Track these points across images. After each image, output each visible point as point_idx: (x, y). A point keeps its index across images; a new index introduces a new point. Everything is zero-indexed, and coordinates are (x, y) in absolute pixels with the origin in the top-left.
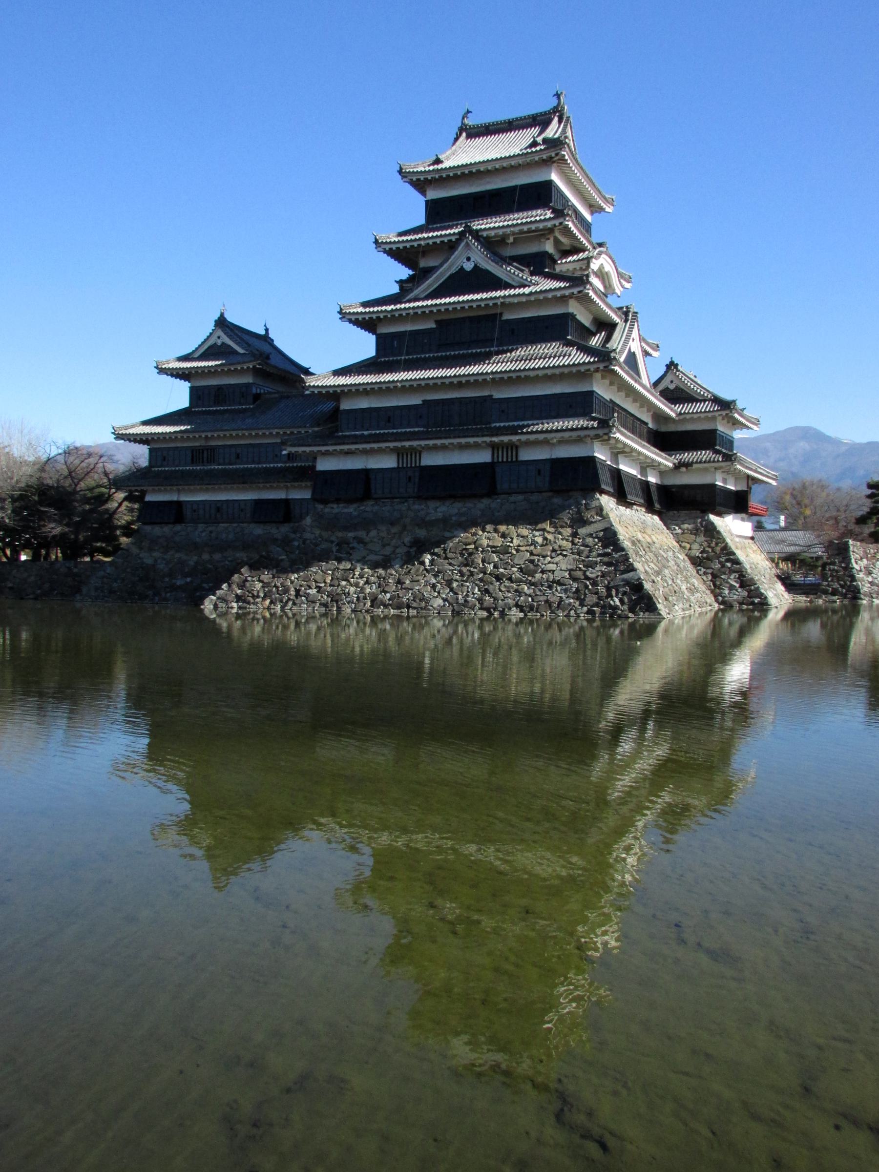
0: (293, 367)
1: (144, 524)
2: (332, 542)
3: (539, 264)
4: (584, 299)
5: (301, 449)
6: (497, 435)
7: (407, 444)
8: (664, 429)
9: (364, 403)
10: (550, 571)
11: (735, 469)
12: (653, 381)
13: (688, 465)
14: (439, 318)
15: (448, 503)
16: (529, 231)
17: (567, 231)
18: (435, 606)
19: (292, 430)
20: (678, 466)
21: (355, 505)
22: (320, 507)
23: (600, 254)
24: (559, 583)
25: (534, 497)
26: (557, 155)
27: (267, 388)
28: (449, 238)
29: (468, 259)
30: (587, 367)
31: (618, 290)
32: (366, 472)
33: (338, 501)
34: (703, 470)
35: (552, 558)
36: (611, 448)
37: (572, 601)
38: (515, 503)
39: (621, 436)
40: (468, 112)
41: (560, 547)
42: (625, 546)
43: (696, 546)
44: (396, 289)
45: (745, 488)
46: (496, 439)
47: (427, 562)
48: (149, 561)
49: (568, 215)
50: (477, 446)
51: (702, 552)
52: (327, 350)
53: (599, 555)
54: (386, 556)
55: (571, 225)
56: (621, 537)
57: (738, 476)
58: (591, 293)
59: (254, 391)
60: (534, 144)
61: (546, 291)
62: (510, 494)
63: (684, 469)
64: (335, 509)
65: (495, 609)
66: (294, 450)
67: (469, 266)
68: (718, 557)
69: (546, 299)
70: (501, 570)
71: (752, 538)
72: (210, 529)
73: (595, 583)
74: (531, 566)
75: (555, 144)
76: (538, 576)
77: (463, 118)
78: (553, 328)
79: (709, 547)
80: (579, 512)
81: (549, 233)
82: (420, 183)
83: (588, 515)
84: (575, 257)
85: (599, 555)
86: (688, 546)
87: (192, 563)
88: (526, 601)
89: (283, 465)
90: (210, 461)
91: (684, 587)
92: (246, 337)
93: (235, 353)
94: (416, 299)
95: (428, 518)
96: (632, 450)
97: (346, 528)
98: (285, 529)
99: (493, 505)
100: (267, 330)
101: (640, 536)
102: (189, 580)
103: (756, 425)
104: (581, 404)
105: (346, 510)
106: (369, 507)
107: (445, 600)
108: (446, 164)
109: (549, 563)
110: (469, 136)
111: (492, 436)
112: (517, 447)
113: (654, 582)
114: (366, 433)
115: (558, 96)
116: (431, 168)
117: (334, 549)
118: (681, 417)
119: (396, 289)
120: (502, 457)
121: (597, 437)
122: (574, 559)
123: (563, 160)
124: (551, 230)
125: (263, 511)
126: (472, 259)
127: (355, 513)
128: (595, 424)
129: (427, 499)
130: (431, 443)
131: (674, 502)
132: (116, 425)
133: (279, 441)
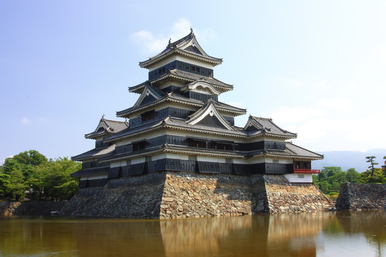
14: (142, 113)
21: (117, 180)
24: (144, 206)
25: (155, 174)
26: (174, 52)
32: (121, 168)
38: (150, 176)
40: (171, 39)
45: (292, 163)
48: (77, 200)
50: (140, 157)
66: (102, 161)
67: (148, 94)
82: (147, 67)
86: (254, 188)
105: (115, 181)
106: (121, 180)
111: (139, 153)
118: (250, 137)
120: (148, 161)
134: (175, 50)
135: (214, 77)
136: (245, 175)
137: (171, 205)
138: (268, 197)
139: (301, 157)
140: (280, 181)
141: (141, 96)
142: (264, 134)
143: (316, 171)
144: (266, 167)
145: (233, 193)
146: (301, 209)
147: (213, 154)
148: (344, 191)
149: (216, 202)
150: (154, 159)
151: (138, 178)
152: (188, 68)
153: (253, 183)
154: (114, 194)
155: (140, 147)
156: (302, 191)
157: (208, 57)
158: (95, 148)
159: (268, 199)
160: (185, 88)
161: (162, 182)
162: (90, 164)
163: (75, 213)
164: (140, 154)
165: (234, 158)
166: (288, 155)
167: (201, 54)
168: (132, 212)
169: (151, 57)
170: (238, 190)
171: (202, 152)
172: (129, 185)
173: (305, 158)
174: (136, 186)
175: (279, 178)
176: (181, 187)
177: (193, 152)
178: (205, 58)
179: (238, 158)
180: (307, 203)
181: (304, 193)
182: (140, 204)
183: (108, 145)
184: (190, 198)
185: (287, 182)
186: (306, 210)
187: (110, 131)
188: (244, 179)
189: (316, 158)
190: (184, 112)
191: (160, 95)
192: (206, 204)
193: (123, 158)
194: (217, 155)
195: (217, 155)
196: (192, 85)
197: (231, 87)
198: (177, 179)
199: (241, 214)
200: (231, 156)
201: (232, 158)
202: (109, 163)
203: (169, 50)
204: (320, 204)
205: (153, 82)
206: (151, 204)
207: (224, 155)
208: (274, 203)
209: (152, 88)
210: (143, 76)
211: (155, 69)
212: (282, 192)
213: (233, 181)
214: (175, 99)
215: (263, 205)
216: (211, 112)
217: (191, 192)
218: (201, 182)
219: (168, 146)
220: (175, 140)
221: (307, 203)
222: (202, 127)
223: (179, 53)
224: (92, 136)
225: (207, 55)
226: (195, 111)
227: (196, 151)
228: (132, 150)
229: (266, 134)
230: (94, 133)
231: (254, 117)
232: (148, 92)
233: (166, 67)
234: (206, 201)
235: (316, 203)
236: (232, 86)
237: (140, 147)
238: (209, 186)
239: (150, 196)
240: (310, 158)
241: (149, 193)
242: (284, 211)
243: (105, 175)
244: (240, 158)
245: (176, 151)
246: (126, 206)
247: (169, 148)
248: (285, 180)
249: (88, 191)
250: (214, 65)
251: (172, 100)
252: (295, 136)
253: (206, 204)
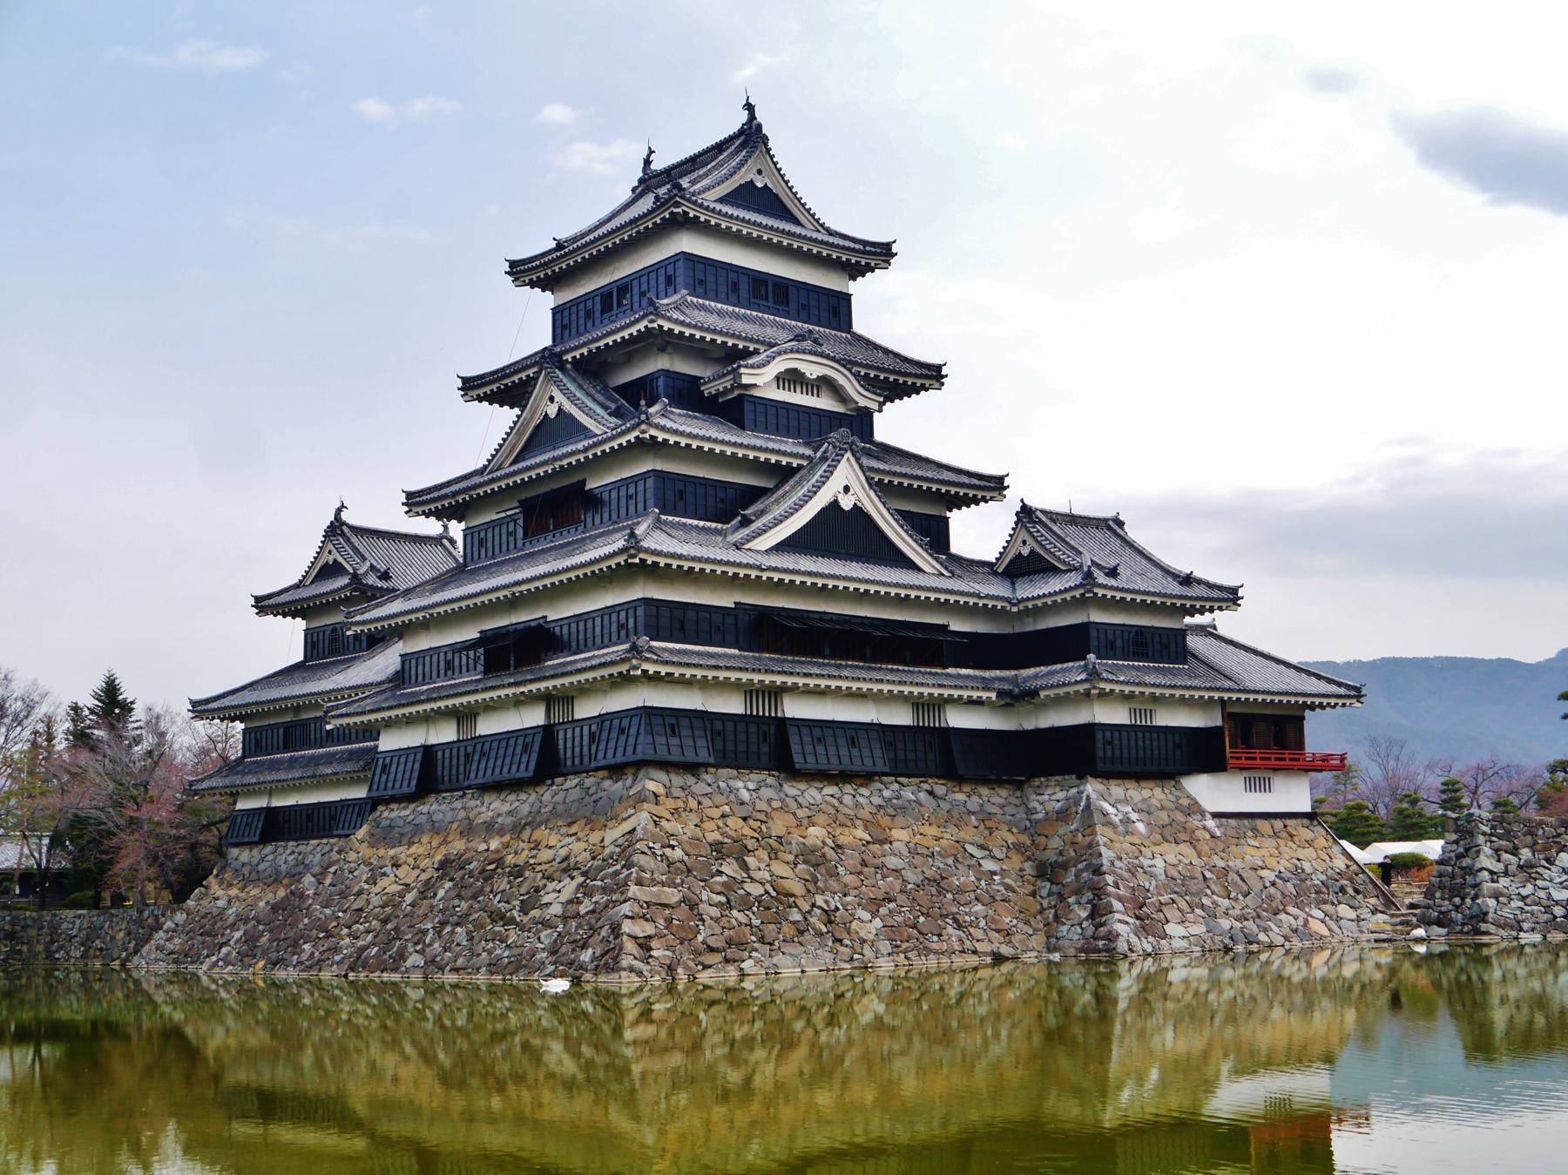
14: (523, 496)
21: (412, 806)
24: (546, 924)
25: (589, 781)
32: (428, 751)
33: (394, 799)
40: (651, 152)
45: (1219, 723)
47: (441, 893)
48: (221, 903)
50: (519, 702)
54: (407, 885)
60: (657, 198)
62: (565, 775)
66: (339, 722)
67: (552, 411)
72: (301, 848)
76: (535, 913)
82: (546, 284)
87: (262, 904)
100: (446, 527)
105: (404, 813)
106: (432, 807)
111: (516, 684)
115: (749, 107)
120: (556, 718)
133: (321, 714)
134: (677, 205)
135: (858, 327)
136: (1000, 782)
137: (669, 921)
138: (1110, 879)
139: (1260, 698)
140: (1163, 808)
141: (519, 417)
142: (1090, 591)
143: (1326, 758)
144: (1100, 745)
145: (950, 861)
146: (1262, 937)
147: (855, 686)
148: (1461, 850)
149: (874, 906)
150: (586, 709)
151: (513, 797)
152: (735, 287)
153: (1040, 816)
154: (401, 872)
155: (516, 651)
156: (1264, 852)
157: (831, 239)
158: (301, 658)
159: (1110, 889)
160: (726, 383)
161: (625, 815)
163: (215, 965)
164: (522, 689)
165: (951, 700)
166: (1199, 689)
167: (797, 222)
168: (490, 953)
169: (563, 235)
170: (971, 849)
171: (806, 675)
172: (468, 830)
173: (1277, 699)
175: (1158, 792)
176: (714, 836)
177: (768, 679)
178: (816, 241)
179: (971, 702)
180: (1291, 909)
181: (1271, 862)
182: (526, 919)
183: (364, 645)
184: (750, 887)
185: (1194, 809)
186: (1287, 939)
187: (372, 580)
188: (995, 799)
189: (1325, 701)
190: (721, 494)
191: (610, 414)
192: (829, 916)
193: (442, 704)
194: (875, 687)
195: (875, 687)
196: (759, 367)
197: (932, 375)
198: (693, 804)
199: (989, 960)
200: (936, 692)
201: (940, 704)
202: (371, 732)
203: (647, 203)
204: (1353, 915)
205: (577, 354)
206: (578, 915)
207: (906, 689)
208: (1137, 905)
209: (574, 380)
210: (528, 324)
212: (1171, 859)
213: (945, 806)
214: (682, 434)
215: (1087, 919)
216: (847, 489)
217: (760, 860)
218: (801, 813)
219: (650, 649)
220: (682, 623)
221: (1291, 909)
222: (806, 563)
223: (696, 217)
225: (822, 225)
226: (770, 485)
227: (779, 673)
228: (480, 668)
229: (1100, 592)
230: (296, 586)
231: (1043, 512)
232: (553, 399)
233: (636, 283)
234: (826, 902)
235: (1327, 907)
236: (939, 368)
237: (516, 651)
238: (839, 831)
240: (1301, 700)
241: (564, 865)
242: (1184, 944)
243: (354, 781)
244: (979, 703)
245: (688, 672)
246: (458, 929)
247: (656, 662)
248: (1185, 802)
249: (270, 857)
250: (856, 271)
251: (667, 436)
252: (1230, 597)
253: (829, 916)
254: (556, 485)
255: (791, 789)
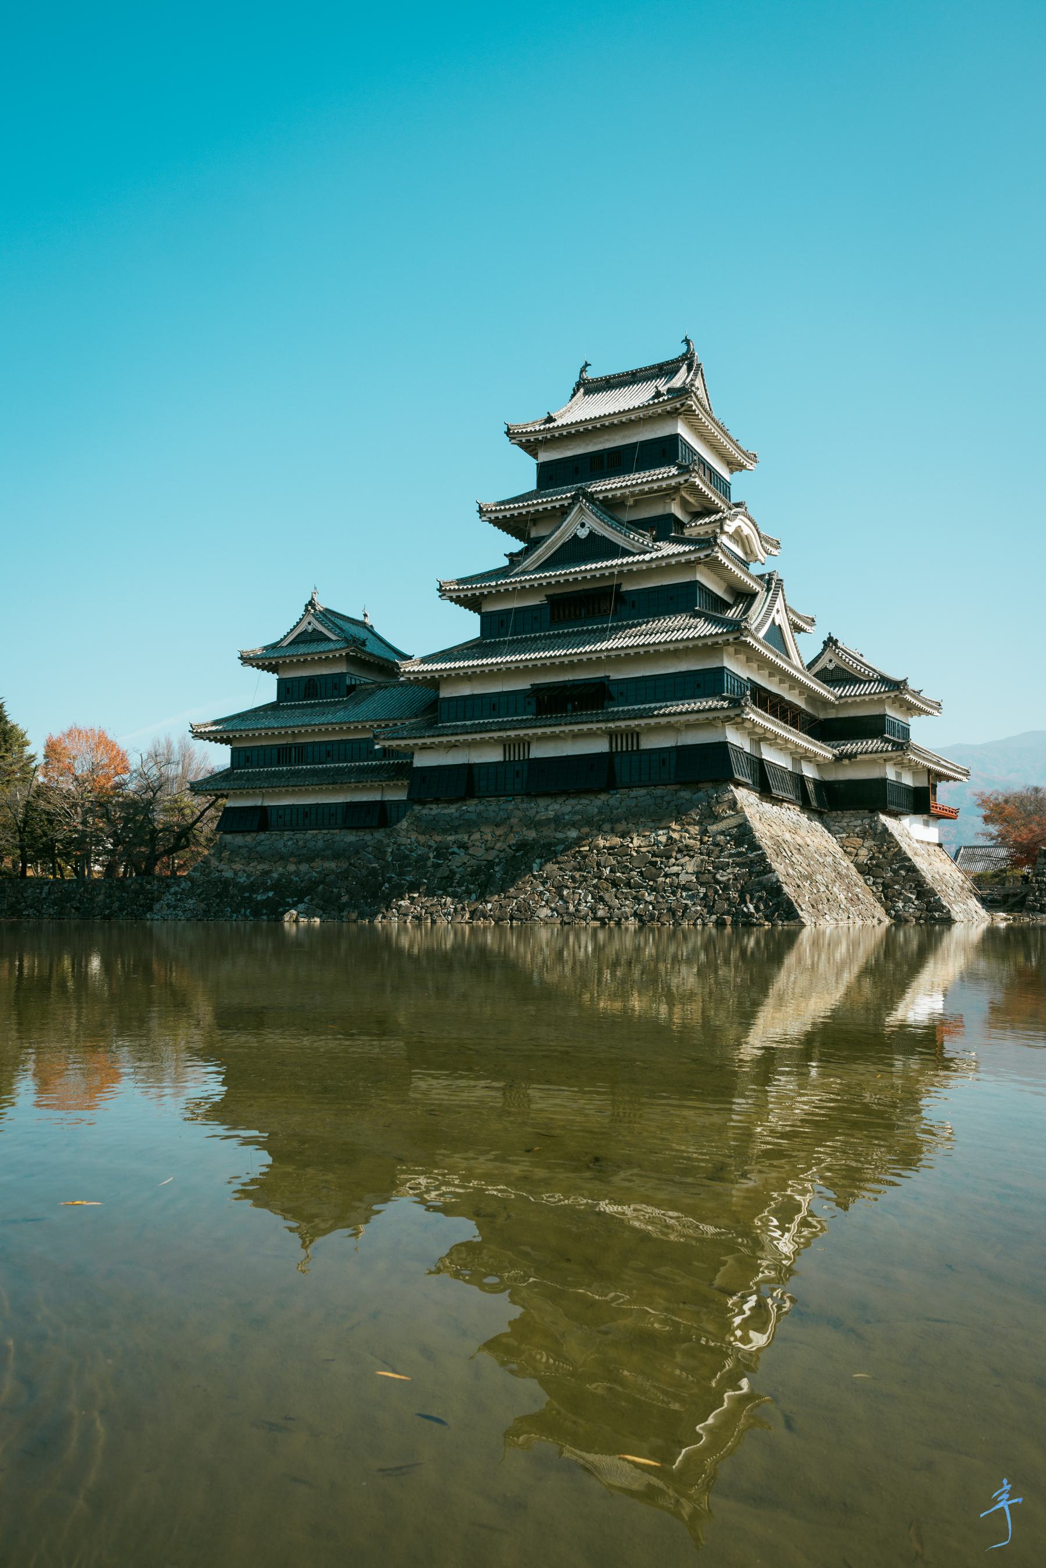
0: (395, 655)
1: (226, 832)
2: (430, 847)
3: (665, 528)
4: (714, 565)
5: (394, 743)
6: (613, 720)
7: (512, 734)
8: (822, 716)
9: (466, 690)
10: (674, 874)
11: (910, 760)
12: (806, 662)
13: (851, 756)
14: (550, 592)
15: (560, 800)
16: (651, 491)
17: (694, 488)
18: (542, 916)
19: (387, 722)
20: (838, 759)
21: (456, 806)
22: (417, 808)
23: (736, 515)
24: (685, 888)
25: (659, 791)
26: (682, 405)
27: (364, 678)
28: (561, 503)
29: (583, 525)
30: (715, 640)
31: (761, 556)
32: (470, 767)
33: (437, 801)
34: (869, 762)
35: (676, 859)
36: (749, 734)
37: (699, 908)
39: (754, 715)
40: (587, 365)
41: (686, 846)
42: (761, 844)
43: (863, 852)
44: (506, 562)
45: (926, 785)
46: (611, 725)
48: (229, 874)
49: (694, 470)
50: (591, 734)
51: (871, 859)
52: (426, 630)
53: (731, 856)
55: (698, 481)
56: (757, 834)
57: (914, 769)
58: (721, 557)
59: (348, 682)
60: (658, 394)
61: (668, 556)
62: (630, 787)
63: (846, 762)
64: (435, 810)
65: (610, 919)
66: (387, 744)
67: (583, 533)
68: (890, 864)
69: (668, 565)
70: (618, 874)
71: (940, 845)
72: (297, 836)
73: (726, 888)
74: (653, 869)
75: (683, 392)
76: (661, 879)
77: (581, 372)
78: (681, 599)
79: (880, 852)
80: (710, 806)
81: (675, 493)
82: (531, 446)
83: (719, 809)
84: (707, 520)
85: (731, 856)
87: (275, 875)
88: (646, 909)
89: (378, 763)
90: (300, 761)
91: (842, 897)
92: (339, 622)
93: (329, 640)
94: (524, 572)
95: (537, 818)
96: (777, 736)
97: (445, 831)
98: (380, 834)
99: (613, 801)
100: (365, 615)
101: (788, 836)
102: (271, 894)
103: (937, 709)
104: (710, 682)
105: (446, 811)
107: (552, 910)
108: (559, 422)
109: (674, 865)
110: (586, 393)
112: (638, 734)
113: (799, 886)
114: (468, 723)
115: (687, 341)
116: (542, 427)
117: (431, 855)
118: (842, 701)
119: (506, 562)
120: (622, 746)
121: (728, 719)
122: (702, 861)
123: (690, 411)
124: (677, 488)
125: (355, 816)
126: (587, 525)
127: (458, 814)
128: (726, 704)
129: (537, 796)
130: (539, 731)
131: (833, 801)
132: (194, 723)
133: (371, 736)
150: (650, 743)
151: (573, 802)
162: (275, 752)
174: (574, 825)
206: (718, 882)
210: (520, 475)
211: (569, 453)
216: (778, 611)
224: (264, 660)
228: (533, 707)
230: (274, 647)
239: (693, 857)
249: (268, 842)
254: (587, 587)
255: (767, 806)
